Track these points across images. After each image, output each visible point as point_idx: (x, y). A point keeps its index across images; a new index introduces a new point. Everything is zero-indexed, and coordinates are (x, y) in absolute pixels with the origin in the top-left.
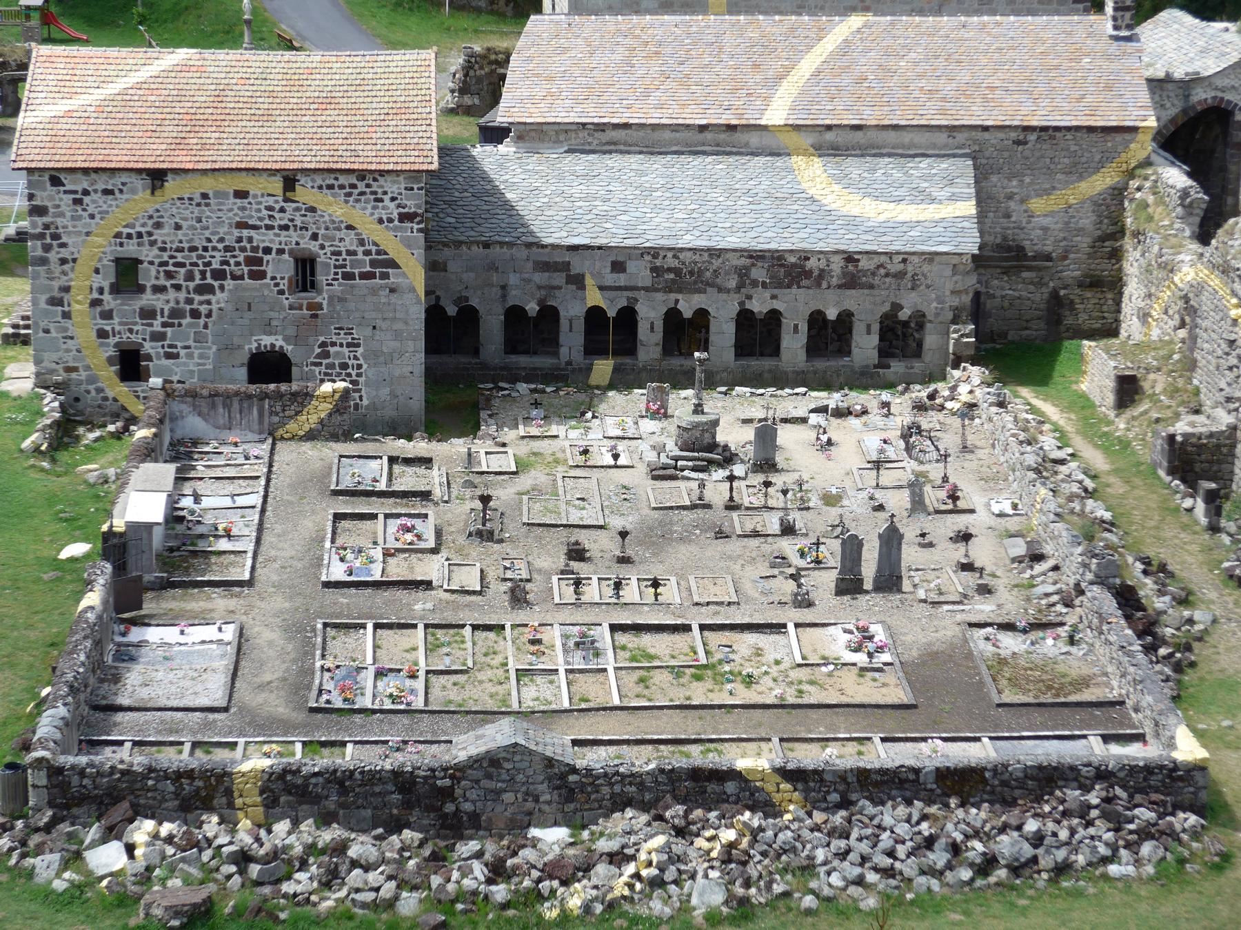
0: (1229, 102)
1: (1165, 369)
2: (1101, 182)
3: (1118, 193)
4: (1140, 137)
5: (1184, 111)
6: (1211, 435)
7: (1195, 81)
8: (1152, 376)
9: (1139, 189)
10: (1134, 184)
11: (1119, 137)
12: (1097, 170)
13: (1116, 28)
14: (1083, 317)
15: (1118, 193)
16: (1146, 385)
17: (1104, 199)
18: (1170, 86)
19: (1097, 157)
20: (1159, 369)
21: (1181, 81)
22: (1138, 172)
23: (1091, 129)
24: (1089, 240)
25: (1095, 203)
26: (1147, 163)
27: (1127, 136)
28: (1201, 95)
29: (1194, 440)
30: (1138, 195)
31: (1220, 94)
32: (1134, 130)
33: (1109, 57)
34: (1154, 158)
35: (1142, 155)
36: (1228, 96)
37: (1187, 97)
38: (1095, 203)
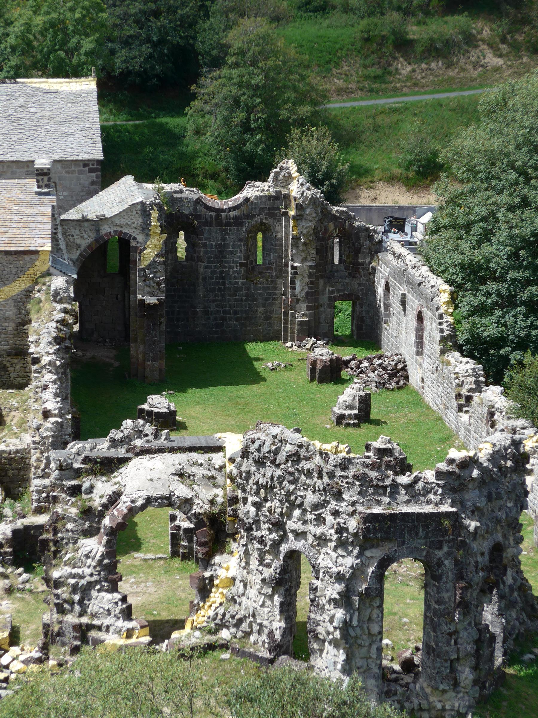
0: (126, 234)
1: (21, 409)
2: (17, 287)
3: (28, 293)
4: (41, 257)
5: (96, 240)
6: (17, 451)
7: (102, 220)
8: (12, 414)
9: (39, 291)
10: (37, 288)
11: (27, 258)
12: (15, 279)
13: (39, 187)
14: (13, 375)
15: (28, 293)
16: (8, 420)
17: (21, 298)
18: (85, 224)
19: (14, 271)
20: (17, 409)
21: (92, 221)
22: (40, 280)
23: (7, 253)
24: (13, 325)
25: (15, 301)
26: (48, 274)
27: (32, 257)
28: (106, 229)
29: (5, 455)
30: (37, 295)
31: (119, 229)
32: (36, 252)
33: (31, 206)
34: (52, 270)
35: (44, 269)
36: (125, 230)
37: (98, 231)
38: (15, 301)
